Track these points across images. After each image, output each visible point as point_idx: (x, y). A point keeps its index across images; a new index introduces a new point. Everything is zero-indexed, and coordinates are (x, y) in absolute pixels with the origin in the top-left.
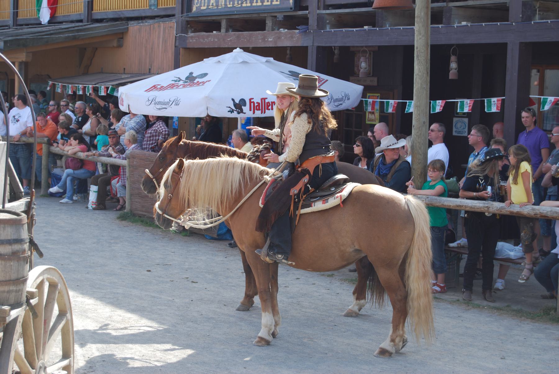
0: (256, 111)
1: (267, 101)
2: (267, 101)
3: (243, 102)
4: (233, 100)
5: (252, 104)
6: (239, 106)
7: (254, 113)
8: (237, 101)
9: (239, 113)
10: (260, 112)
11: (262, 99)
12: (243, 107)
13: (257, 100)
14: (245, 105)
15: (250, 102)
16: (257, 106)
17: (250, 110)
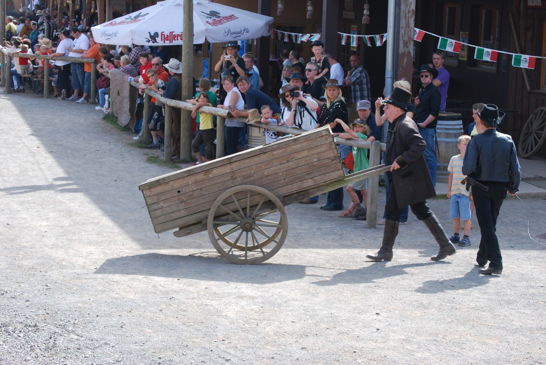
0: (166, 41)
1: (174, 34)
2: (174, 34)
3: (156, 34)
4: (149, 33)
5: (163, 36)
6: (153, 37)
7: (164, 42)
8: (152, 34)
9: (153, 42)
10: (169, 41)
11: (170, 33)
12: (156, 38)
13: (167, 33)
14: (158, 37)
15: (162, 35)
16: (166, 37)
17: (162, 40)
